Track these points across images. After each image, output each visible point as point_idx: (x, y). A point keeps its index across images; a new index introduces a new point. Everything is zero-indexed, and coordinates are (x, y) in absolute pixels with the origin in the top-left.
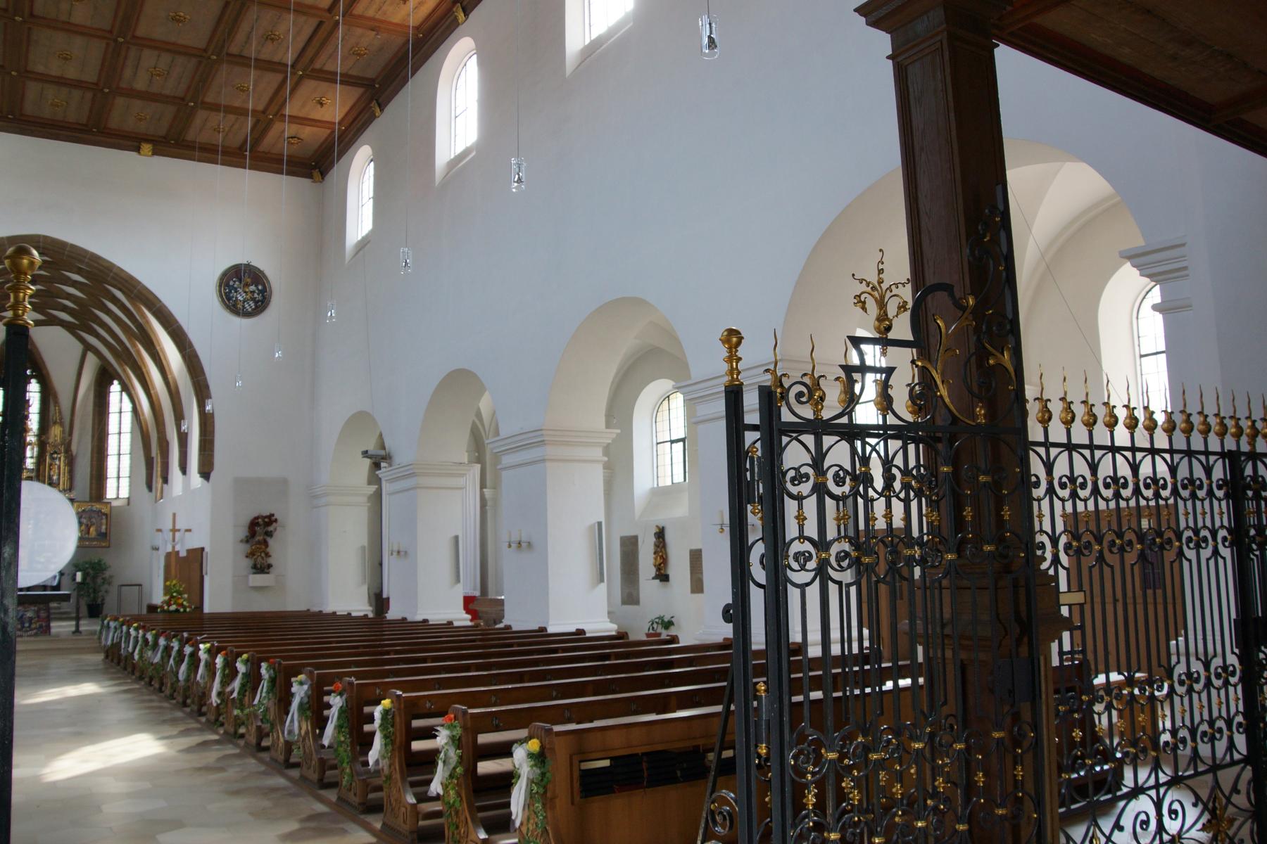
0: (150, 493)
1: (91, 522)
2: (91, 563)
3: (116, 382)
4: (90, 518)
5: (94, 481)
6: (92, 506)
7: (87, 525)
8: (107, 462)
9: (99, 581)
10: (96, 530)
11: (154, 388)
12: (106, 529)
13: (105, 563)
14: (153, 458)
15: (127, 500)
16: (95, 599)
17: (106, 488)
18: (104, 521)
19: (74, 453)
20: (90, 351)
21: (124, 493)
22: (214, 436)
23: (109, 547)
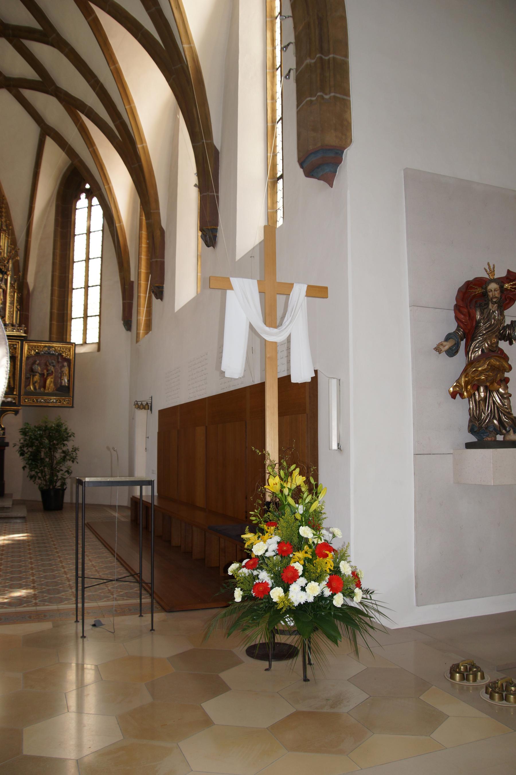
0: (129, 333)
1: (48, 370)
2: (46, 428)
3: (83, 196)
4: (46, 365)
5: (55, 323)
6: (49, 347)
7: (42, 375)
8: (71, 297)
9: (58, 455)
10: (55, 383)
11: (142, 140)
12: (69, 381)
13: (66, 429)
14: (133, 282)
15: (96, 346)
16: (52, 481)
17: (71, 331)
18: (66, 370)
19: (31, 288)
20: (49, 136)
21: (93, 337)
22: (346, 56)
23: (72, 407)
